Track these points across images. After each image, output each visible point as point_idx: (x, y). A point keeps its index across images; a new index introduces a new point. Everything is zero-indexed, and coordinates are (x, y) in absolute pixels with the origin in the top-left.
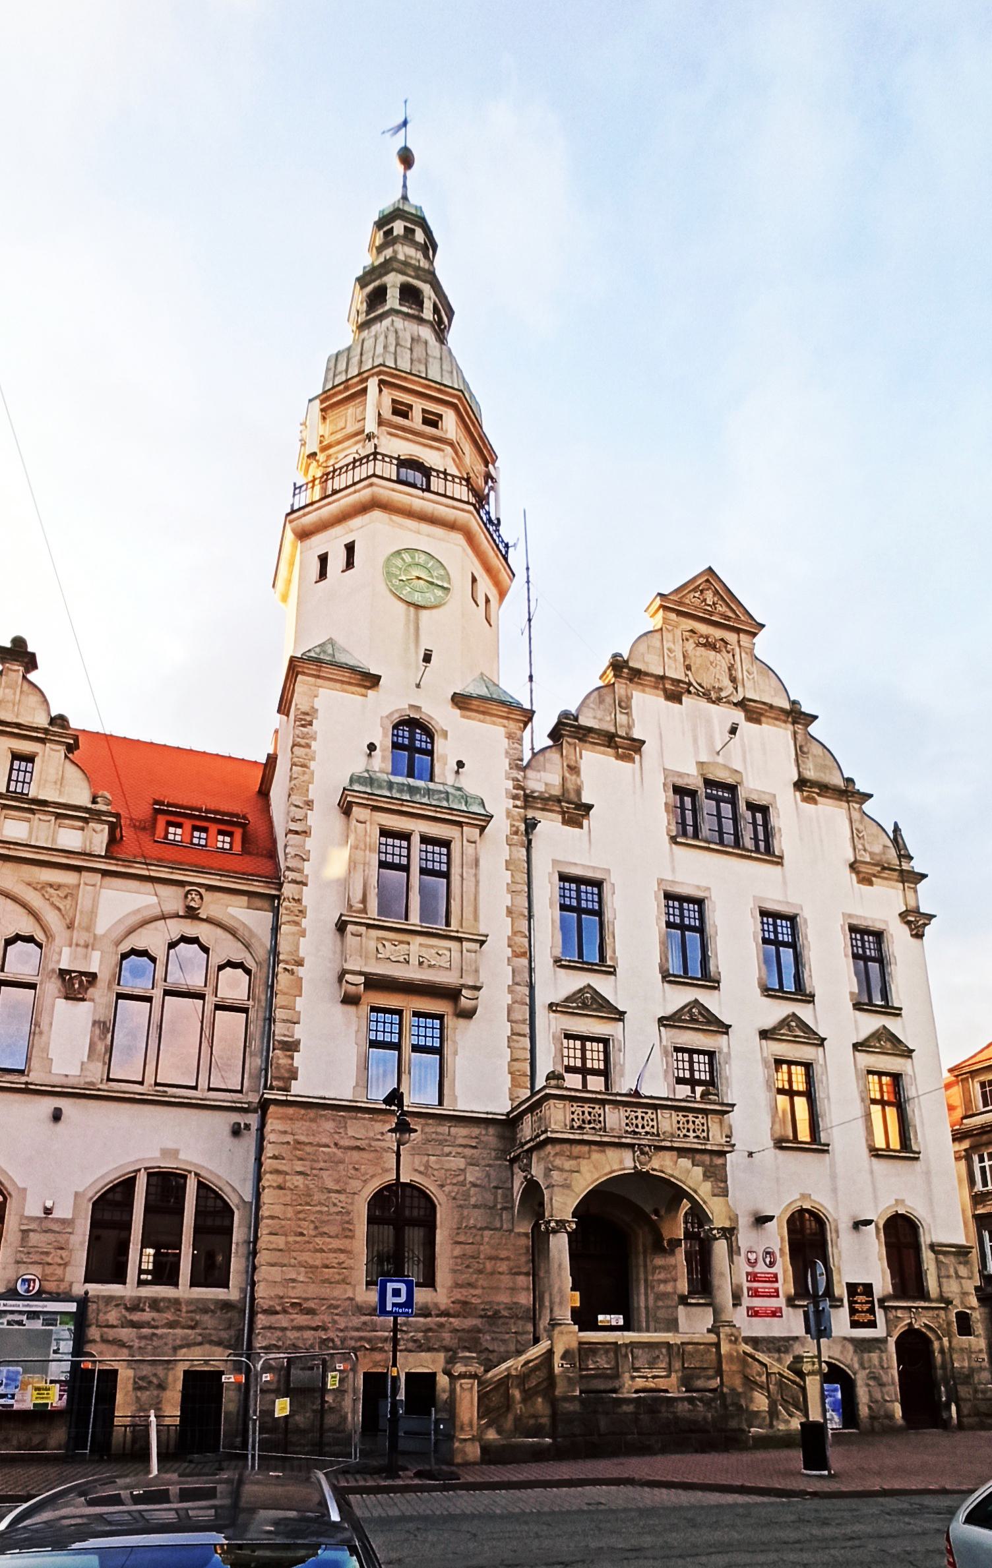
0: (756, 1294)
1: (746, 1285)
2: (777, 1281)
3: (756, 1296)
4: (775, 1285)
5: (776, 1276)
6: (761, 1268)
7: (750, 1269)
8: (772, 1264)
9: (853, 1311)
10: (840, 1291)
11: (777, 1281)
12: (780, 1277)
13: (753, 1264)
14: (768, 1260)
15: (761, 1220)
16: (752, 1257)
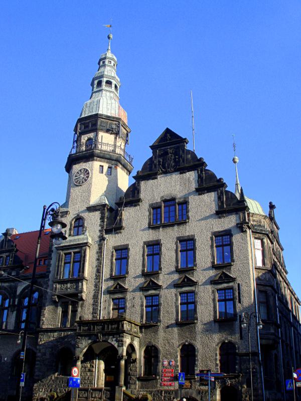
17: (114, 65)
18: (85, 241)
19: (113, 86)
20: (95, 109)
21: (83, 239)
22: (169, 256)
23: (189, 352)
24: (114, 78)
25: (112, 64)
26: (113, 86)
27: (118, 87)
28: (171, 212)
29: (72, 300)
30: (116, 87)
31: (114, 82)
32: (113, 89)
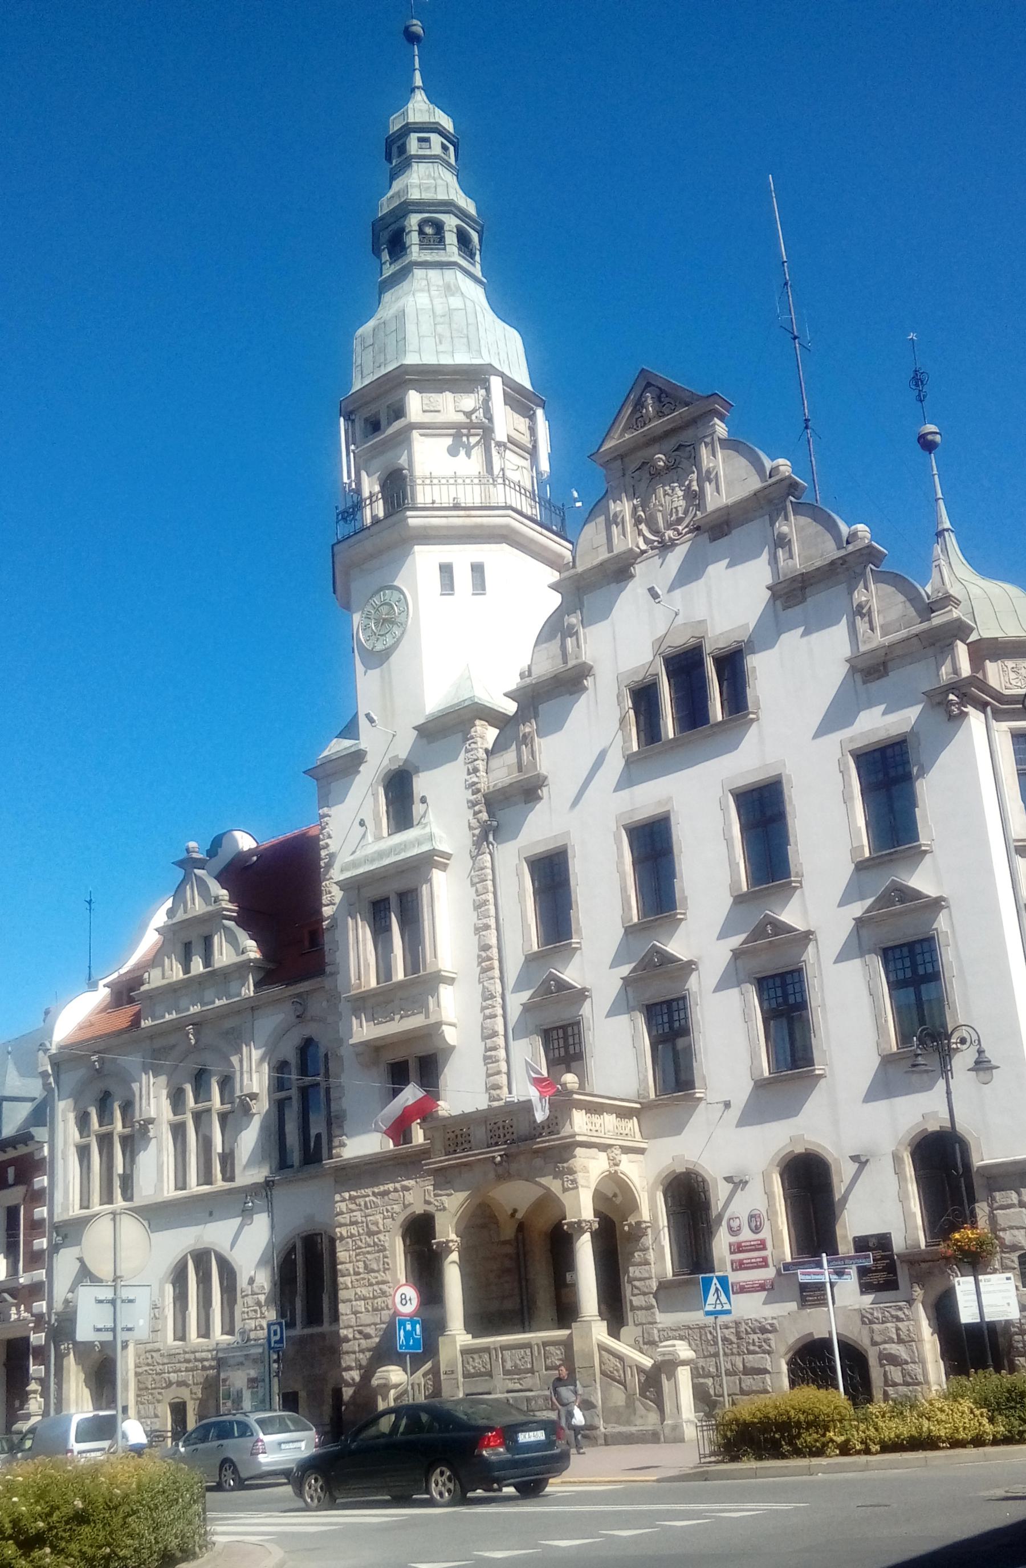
0: (740, 1266)
1: (729, 1258)
2: (764, 1248)
3: (741, 1269)
4: (763, 1253)
5: (762, 1246)
6: (746, 1235)
7: (733, 1239)
8: (756, 1230)
9: (863, 1272)
10: (845, 1247)
11: (764, 1248)
12: (769, 1244)
13: (733, 1232)
14: (753, 1225)
15: (737, 1183)
16: (735, 1224)
17: (445, 148)
18: (425, 848)
19: (451, 238)
20: (391, 349)
21: (419, 842)
22: (710, 860)
23: (809, 1185)
24: (448, 207)
25: (436, 149)
26: (451, 238)
27: (475, 236)
28: (695, 693)
29: (416, 1064)
30: (463, 239)
31: (451, 222)
32: (452, 251)
